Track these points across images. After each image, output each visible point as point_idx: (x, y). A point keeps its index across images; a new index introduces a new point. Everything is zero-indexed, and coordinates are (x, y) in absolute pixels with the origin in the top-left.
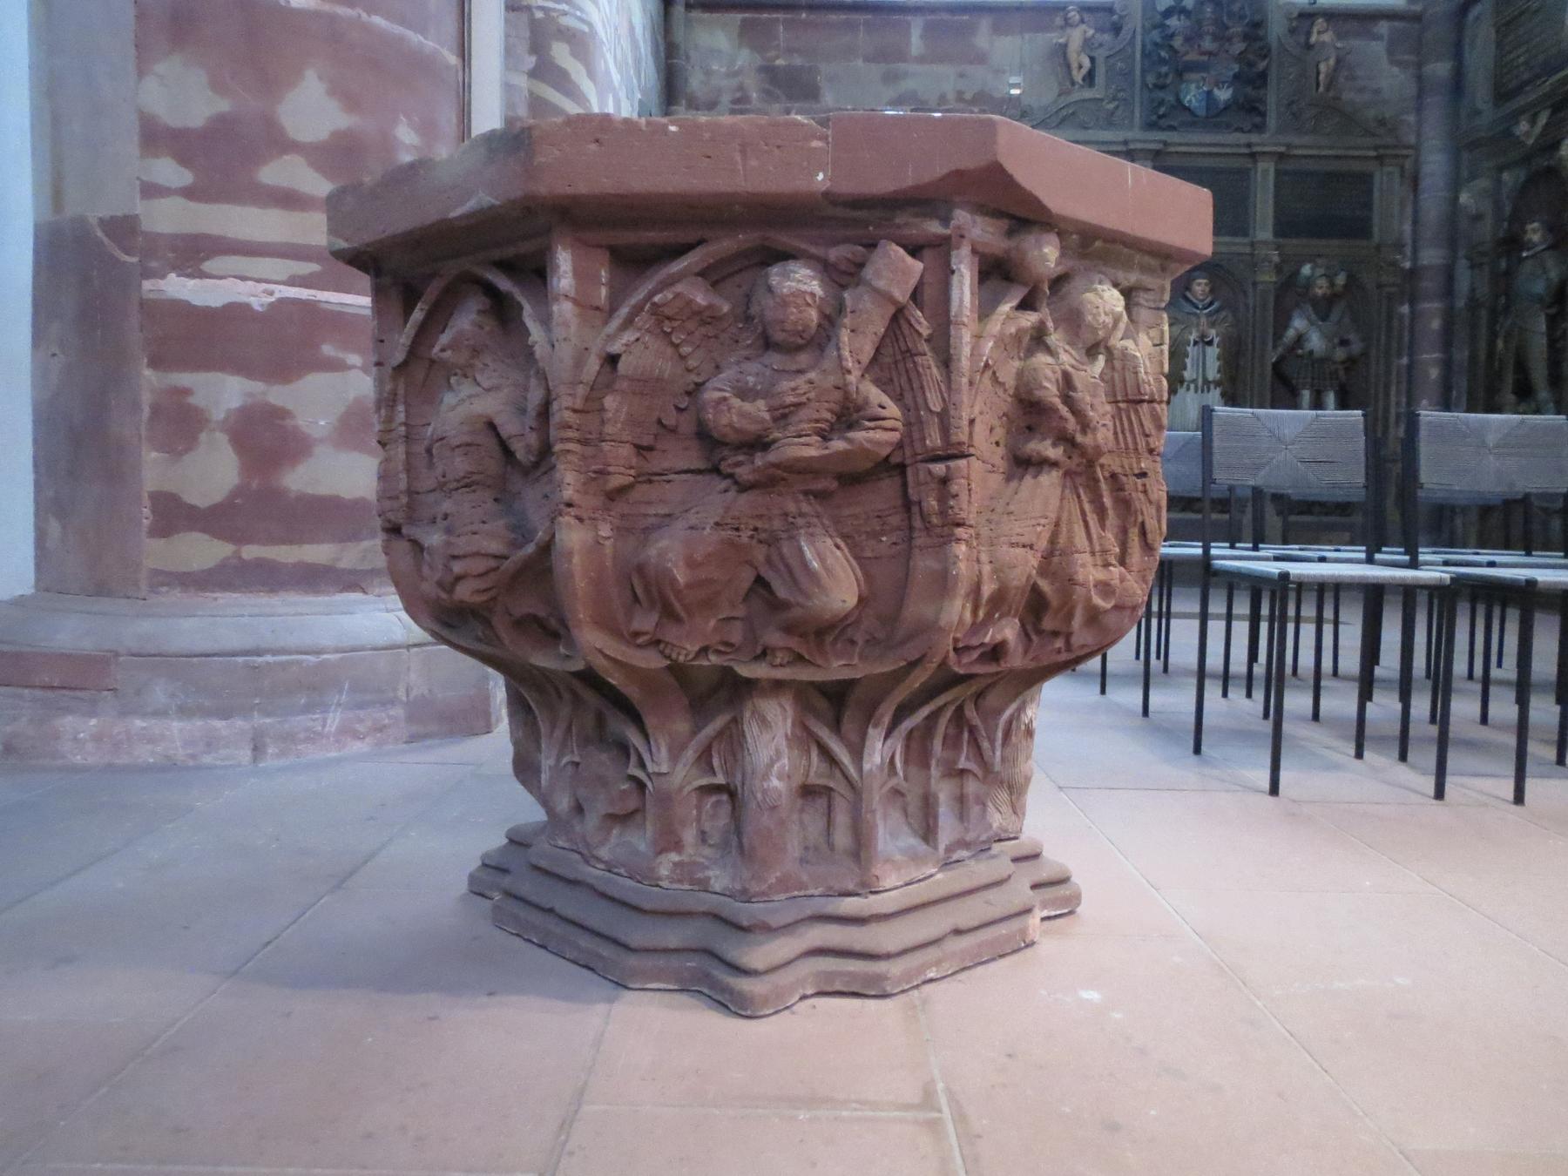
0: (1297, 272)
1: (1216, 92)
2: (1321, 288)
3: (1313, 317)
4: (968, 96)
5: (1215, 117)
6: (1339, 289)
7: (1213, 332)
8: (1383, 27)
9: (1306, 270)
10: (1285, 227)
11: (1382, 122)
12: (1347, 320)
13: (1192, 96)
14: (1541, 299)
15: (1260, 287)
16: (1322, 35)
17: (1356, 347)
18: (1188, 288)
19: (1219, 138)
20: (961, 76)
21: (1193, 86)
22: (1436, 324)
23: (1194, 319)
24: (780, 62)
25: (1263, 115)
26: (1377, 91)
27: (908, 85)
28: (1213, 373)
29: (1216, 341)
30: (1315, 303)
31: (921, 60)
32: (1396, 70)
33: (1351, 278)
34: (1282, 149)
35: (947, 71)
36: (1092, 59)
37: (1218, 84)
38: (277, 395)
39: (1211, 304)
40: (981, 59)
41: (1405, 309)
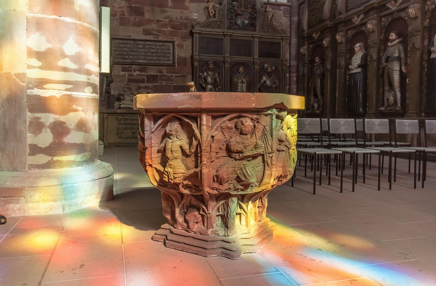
0: (264, 66)
1: (245, 21)
2: (269, 70)
4: (183, 18)
5: (244, 27)
7: (244, 80)
8: (282, 8)
9: (266, 65)
10: (261, 55)
11: (282, 31)
12: (275, 78)
13: (239, 22)
14: (319, 75)
15: (255, 69)
16: (269, 9)
17: (278, 84)
18: (238, 69)
19: (245, 32)
20: (182, 12)
21: (239, 19)
22: (295, 79)
23: (240, 77)
24: (133, 5)
25: (255, 27)
26: (281, 23)
27: (168, 14)
30: (268, 73)
31: (171, 8)
32: (285, 18)
34: (260, 36)
35: (178, 11)
36: (215, 11)
37: (245, 19)
38: (62, 118)
39: (244, 73)
40: (187, 8)
41: (288, 75)
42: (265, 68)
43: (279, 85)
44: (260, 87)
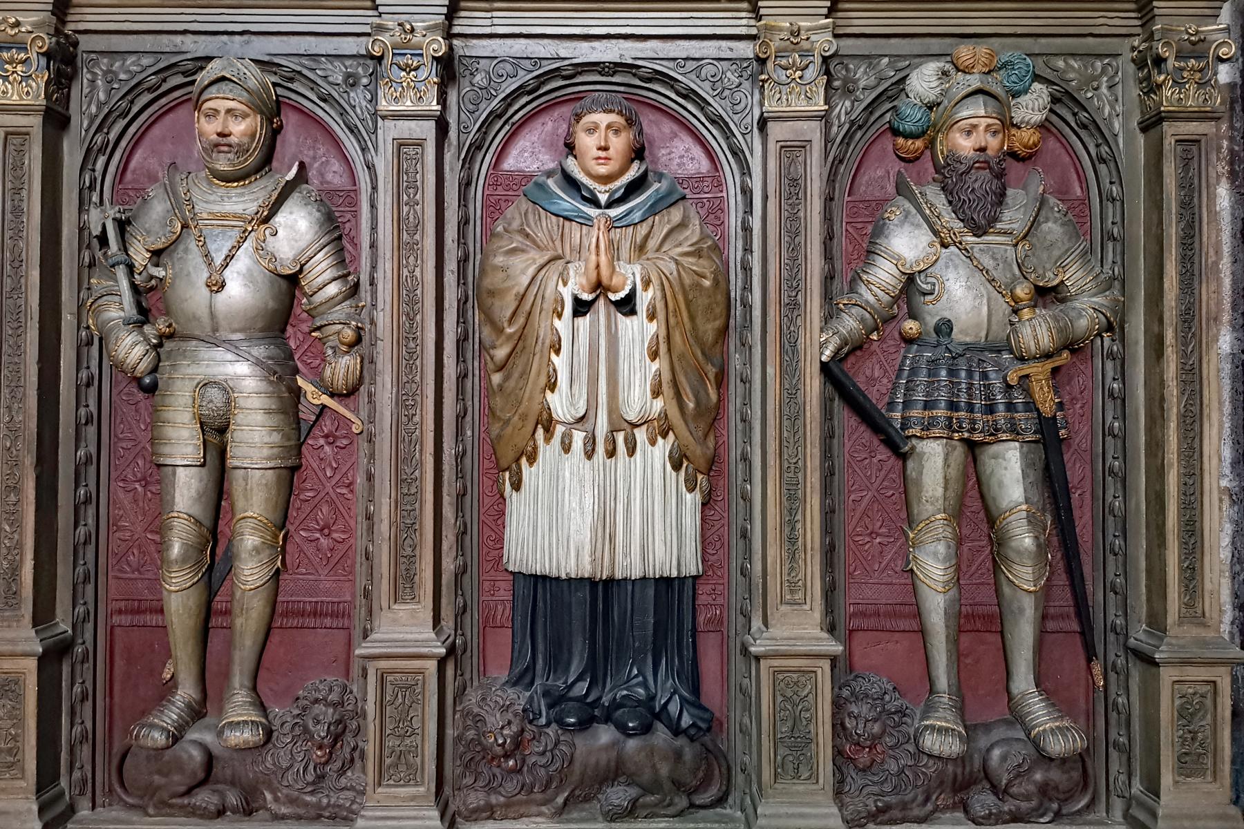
3: (949, 219)
6: (1027, 136)
9: (924, 82)
12: (1052, 229)
15: (775, 130)
17: (1086, 310)
28: (638, 399)
29: (644, 299)
30: (950, 175)
33: (1062, 98)
42: (912, 117)
43: (1114, 326)
44: (854, 348)
